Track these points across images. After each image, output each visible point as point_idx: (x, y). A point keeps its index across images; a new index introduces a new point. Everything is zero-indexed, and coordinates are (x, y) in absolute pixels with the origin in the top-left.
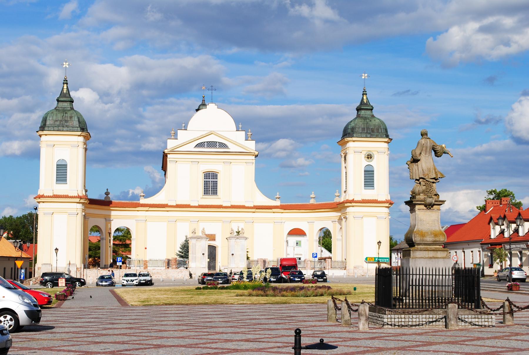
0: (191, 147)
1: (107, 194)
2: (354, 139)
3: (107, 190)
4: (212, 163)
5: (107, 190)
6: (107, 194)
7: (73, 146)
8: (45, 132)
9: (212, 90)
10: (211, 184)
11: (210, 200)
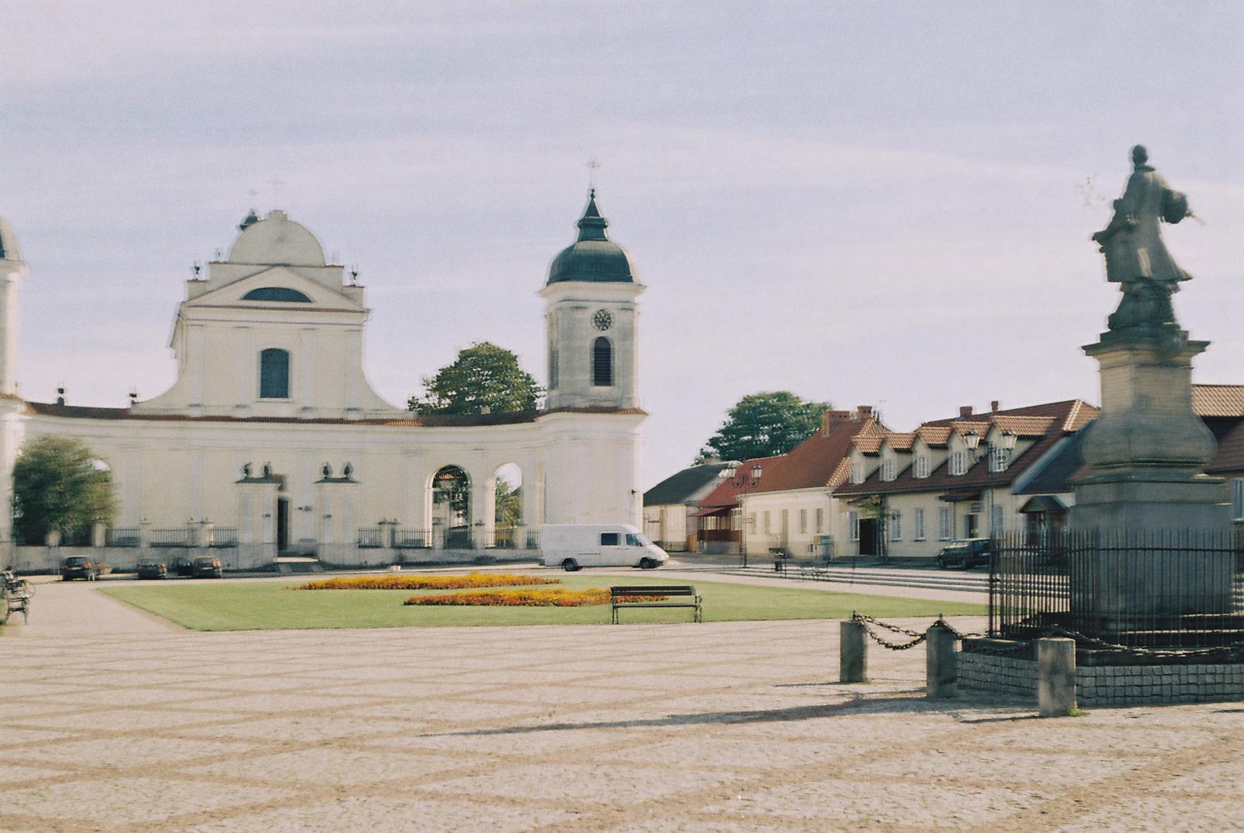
4: (275, 328)
10: (275, 371)
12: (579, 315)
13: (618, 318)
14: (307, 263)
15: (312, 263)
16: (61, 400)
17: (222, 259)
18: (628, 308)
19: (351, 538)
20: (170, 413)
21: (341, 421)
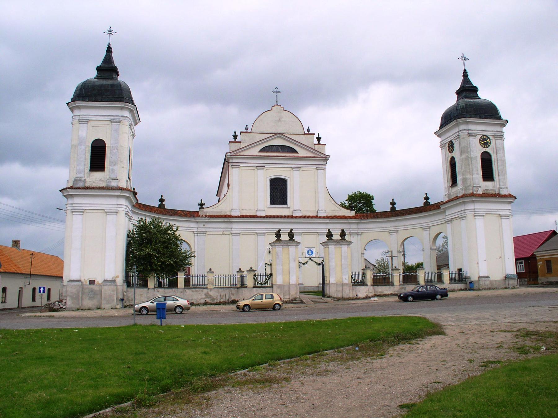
0: (255, 151)
1: (162, 200)
2: (469, 120)
3: (162, 196)
5: (162, 196)
6: (162, 200)
7: (112, 121)
8: (78, 103)
9: (277, 92)
10: (278, 191)
11: (278, 210)
12: (471, 139)
13: (493, 141)
14: (295, 132)
15: (298, 132)
16: (162, 206)
17: (249, 131)
18: (501, 136)
19: (347, 279)
20: (223, 214)
21: (316, 217)
